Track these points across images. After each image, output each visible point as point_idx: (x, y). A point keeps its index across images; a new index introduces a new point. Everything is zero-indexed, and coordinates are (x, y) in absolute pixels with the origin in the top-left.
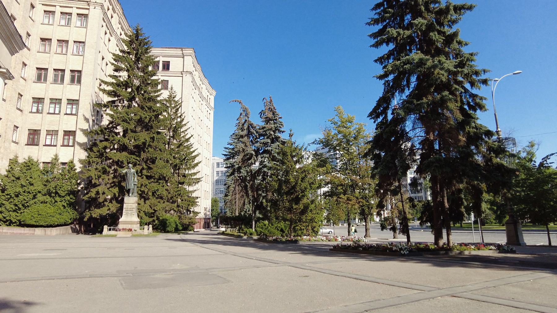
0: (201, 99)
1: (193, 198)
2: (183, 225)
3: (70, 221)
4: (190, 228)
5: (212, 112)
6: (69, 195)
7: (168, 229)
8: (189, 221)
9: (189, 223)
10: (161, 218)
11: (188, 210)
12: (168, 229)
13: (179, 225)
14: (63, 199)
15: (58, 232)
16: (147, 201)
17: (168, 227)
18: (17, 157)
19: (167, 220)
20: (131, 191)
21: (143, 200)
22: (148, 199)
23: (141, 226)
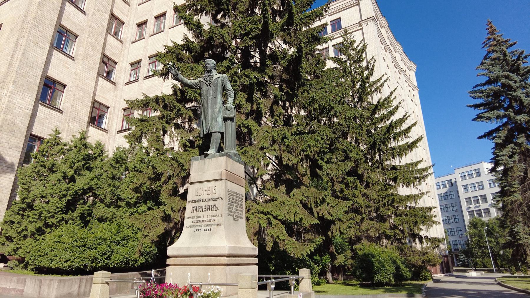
0: (397, 70)
1: (421, 209)
2: (411, 266)
3: (141, 260)
4: (424, 273)
5: (416, 93)
6: (145, 202)
7: (380, 278)
8: (423, 258)
9: (423, 262)
10: (360, 253)
11: (414, 236)
12: (380, 278)
13: (402, 267)
14: (133, 210)
15: (65, 291)
16: (295, 191)
17: (379, 271)
18: (57, 132)
19: (373, 256)
20: (215, 139)
21: (283, 188)
22: (299, 185)
23: (263, 269)
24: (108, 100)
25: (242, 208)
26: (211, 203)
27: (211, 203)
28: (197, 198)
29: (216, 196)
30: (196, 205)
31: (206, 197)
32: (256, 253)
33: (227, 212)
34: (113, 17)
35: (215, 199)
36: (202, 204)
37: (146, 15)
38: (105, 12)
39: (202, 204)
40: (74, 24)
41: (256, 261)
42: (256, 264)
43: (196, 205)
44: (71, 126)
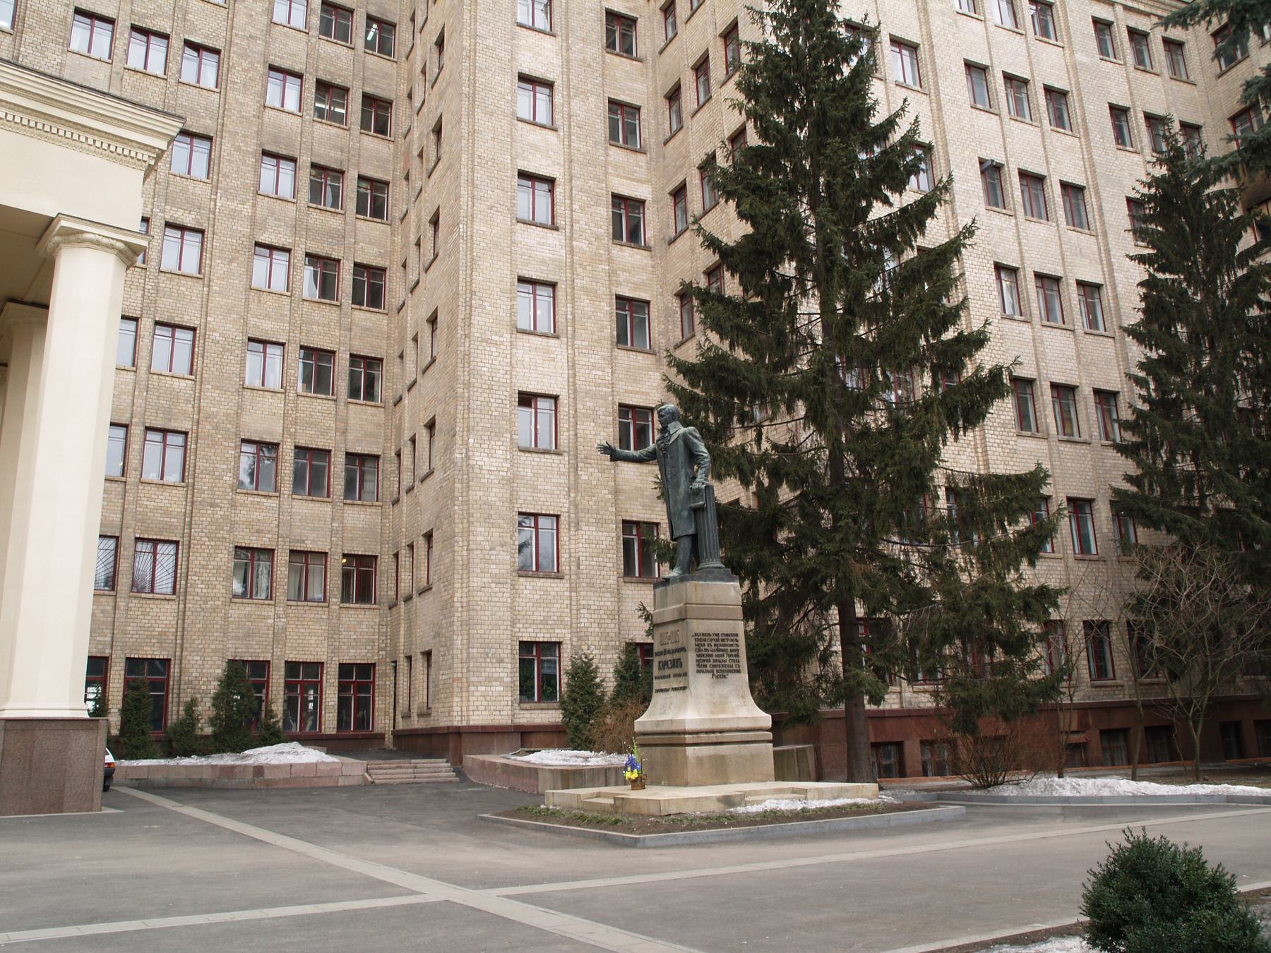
24: (648, 394)
25: (737, 656)
26: (676, 656)
27: (676, 656)
28: (662, 649)
29: (679, 645)
30: (663, 658)
31: (670, 647)
32: (769, 724)
33: (696, 668)
34: (618, 199)
35: (678, 650)
36: (668, 657)
37: (681, 167)
38: (597, 204)
39: (668, 657)
40: (544, 262)
41: (770, 735)
42: (769, 742)
43: (663, 658)
44: (585, 477)
